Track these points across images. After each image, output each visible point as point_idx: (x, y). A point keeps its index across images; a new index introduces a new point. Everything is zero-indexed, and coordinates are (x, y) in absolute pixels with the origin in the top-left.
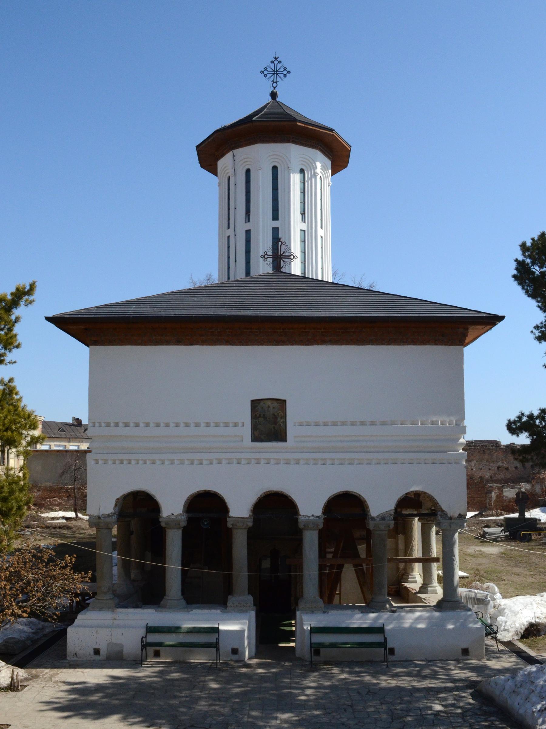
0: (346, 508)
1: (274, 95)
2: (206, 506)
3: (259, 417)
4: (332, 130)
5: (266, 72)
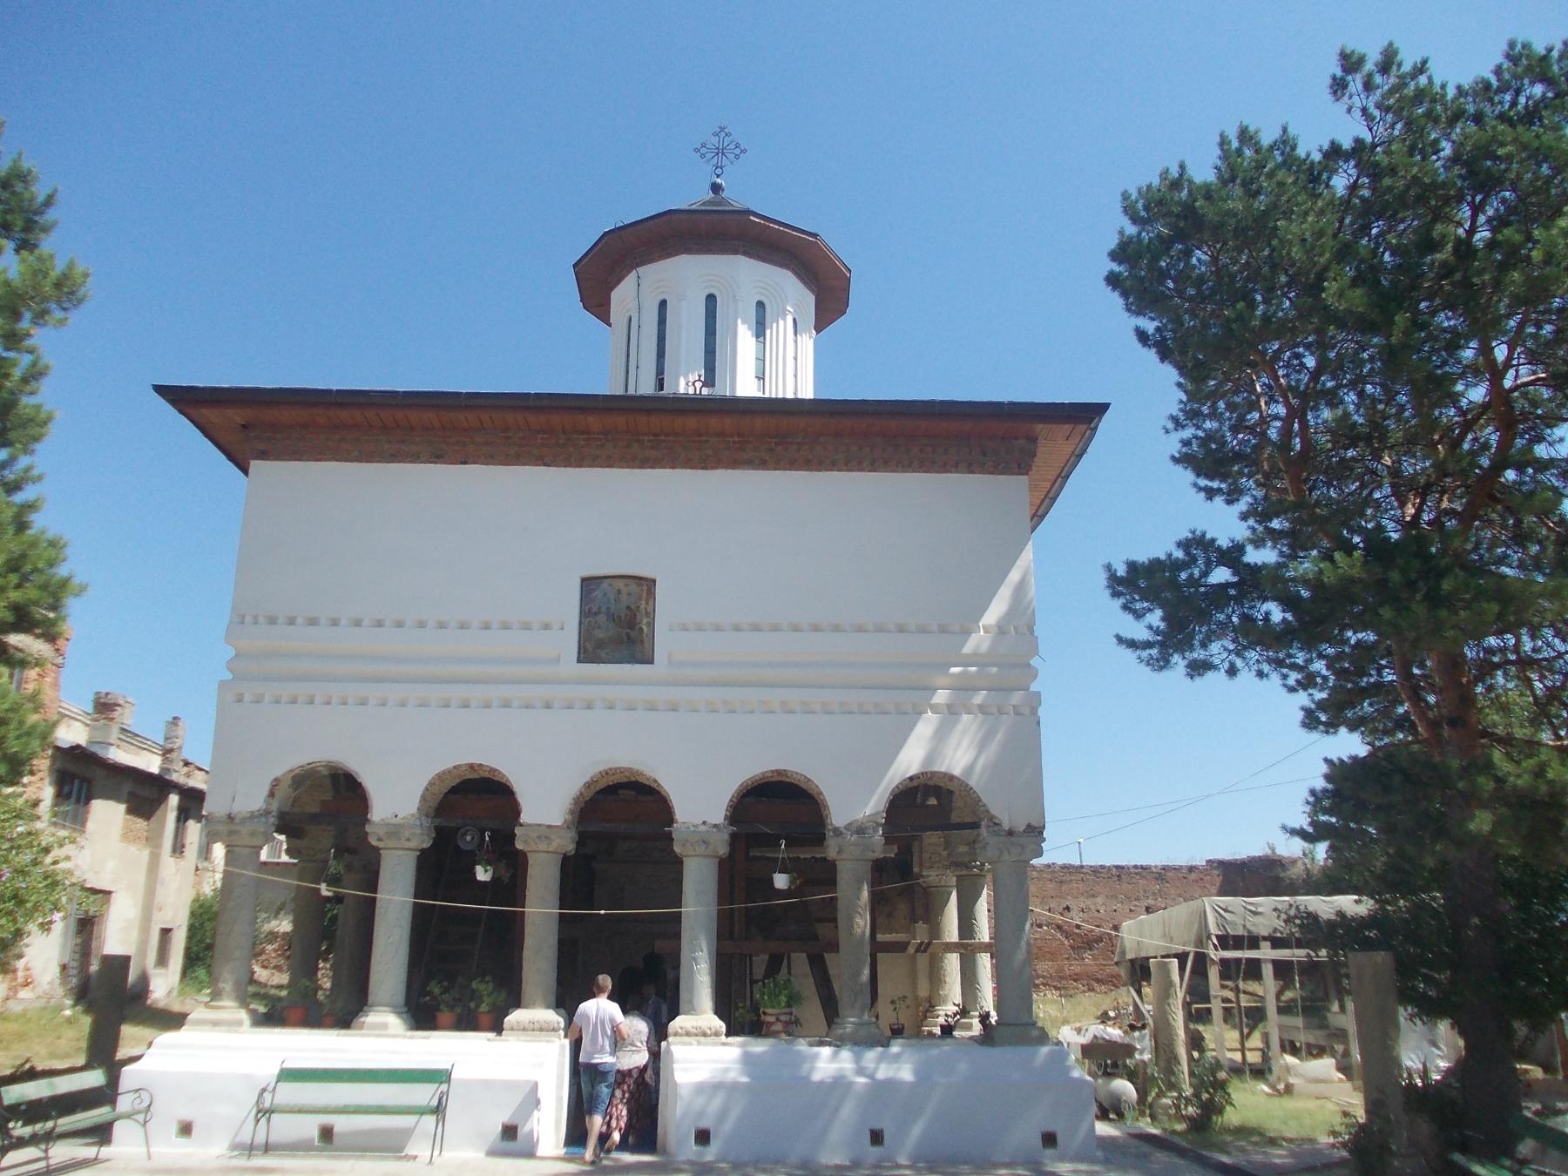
0: (777, 811)
1: (716, 188)
2: (474, 807)
3: (596, 614)
4: (815, 235)
5: (703, 151)
